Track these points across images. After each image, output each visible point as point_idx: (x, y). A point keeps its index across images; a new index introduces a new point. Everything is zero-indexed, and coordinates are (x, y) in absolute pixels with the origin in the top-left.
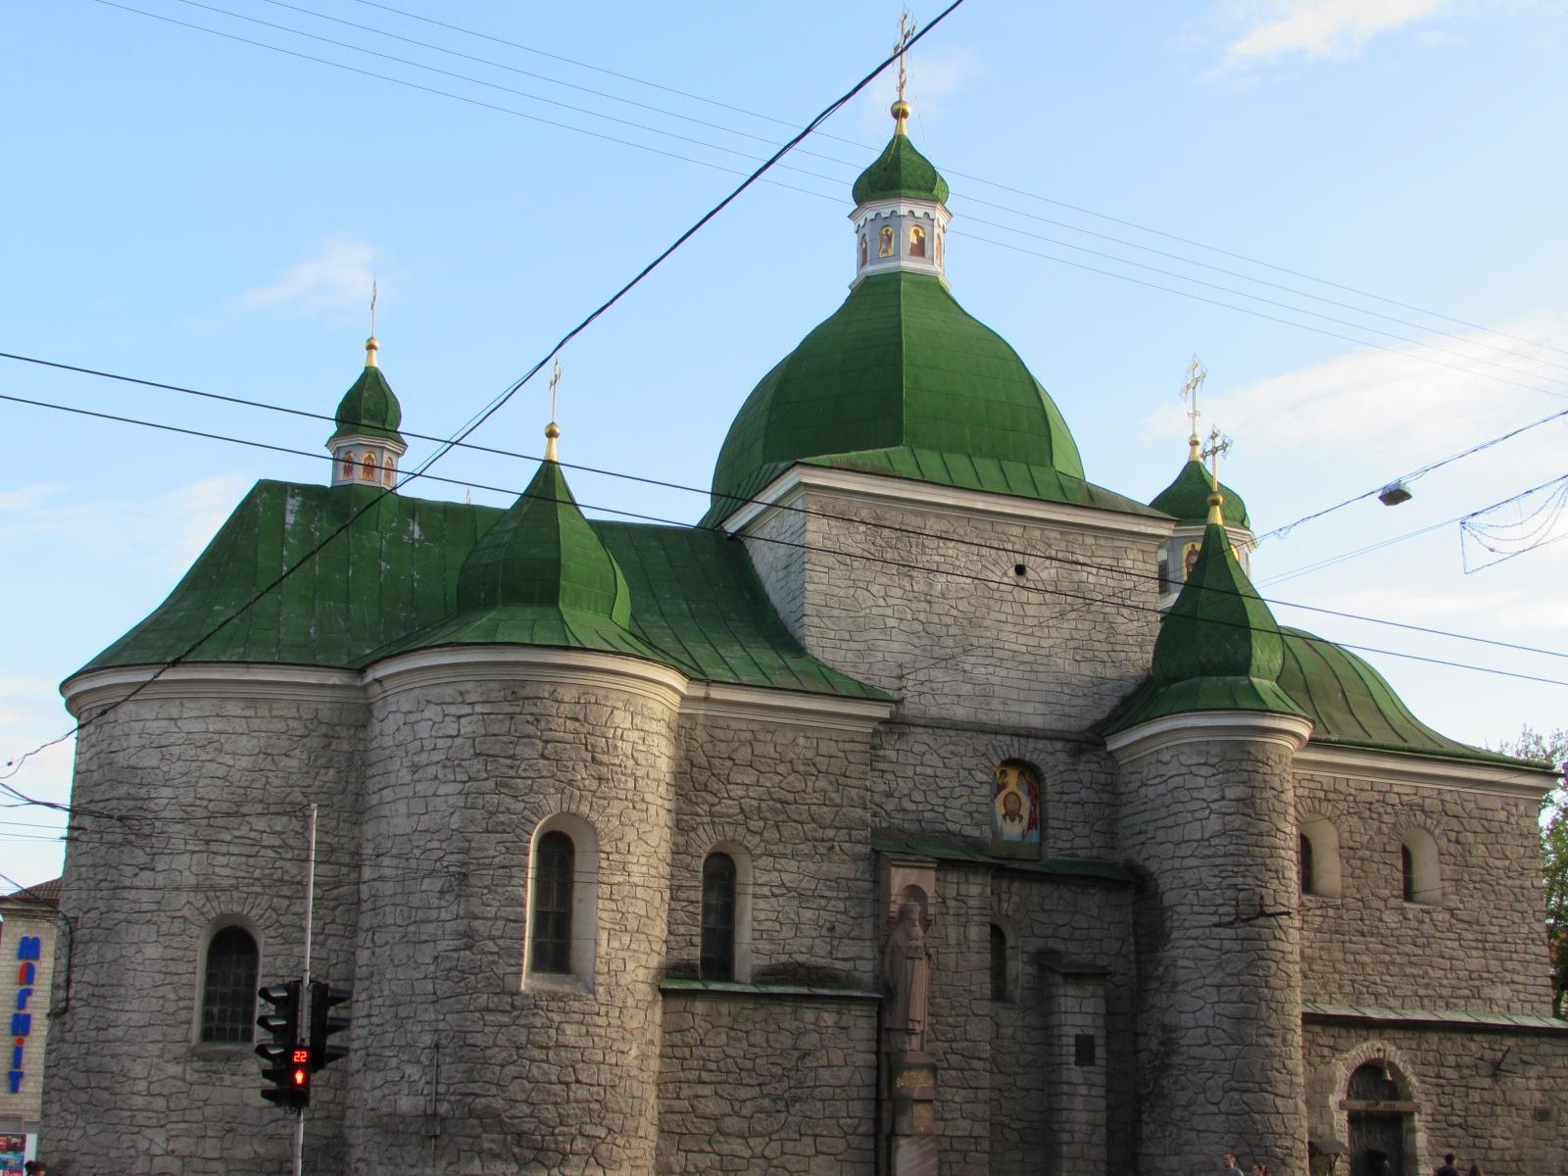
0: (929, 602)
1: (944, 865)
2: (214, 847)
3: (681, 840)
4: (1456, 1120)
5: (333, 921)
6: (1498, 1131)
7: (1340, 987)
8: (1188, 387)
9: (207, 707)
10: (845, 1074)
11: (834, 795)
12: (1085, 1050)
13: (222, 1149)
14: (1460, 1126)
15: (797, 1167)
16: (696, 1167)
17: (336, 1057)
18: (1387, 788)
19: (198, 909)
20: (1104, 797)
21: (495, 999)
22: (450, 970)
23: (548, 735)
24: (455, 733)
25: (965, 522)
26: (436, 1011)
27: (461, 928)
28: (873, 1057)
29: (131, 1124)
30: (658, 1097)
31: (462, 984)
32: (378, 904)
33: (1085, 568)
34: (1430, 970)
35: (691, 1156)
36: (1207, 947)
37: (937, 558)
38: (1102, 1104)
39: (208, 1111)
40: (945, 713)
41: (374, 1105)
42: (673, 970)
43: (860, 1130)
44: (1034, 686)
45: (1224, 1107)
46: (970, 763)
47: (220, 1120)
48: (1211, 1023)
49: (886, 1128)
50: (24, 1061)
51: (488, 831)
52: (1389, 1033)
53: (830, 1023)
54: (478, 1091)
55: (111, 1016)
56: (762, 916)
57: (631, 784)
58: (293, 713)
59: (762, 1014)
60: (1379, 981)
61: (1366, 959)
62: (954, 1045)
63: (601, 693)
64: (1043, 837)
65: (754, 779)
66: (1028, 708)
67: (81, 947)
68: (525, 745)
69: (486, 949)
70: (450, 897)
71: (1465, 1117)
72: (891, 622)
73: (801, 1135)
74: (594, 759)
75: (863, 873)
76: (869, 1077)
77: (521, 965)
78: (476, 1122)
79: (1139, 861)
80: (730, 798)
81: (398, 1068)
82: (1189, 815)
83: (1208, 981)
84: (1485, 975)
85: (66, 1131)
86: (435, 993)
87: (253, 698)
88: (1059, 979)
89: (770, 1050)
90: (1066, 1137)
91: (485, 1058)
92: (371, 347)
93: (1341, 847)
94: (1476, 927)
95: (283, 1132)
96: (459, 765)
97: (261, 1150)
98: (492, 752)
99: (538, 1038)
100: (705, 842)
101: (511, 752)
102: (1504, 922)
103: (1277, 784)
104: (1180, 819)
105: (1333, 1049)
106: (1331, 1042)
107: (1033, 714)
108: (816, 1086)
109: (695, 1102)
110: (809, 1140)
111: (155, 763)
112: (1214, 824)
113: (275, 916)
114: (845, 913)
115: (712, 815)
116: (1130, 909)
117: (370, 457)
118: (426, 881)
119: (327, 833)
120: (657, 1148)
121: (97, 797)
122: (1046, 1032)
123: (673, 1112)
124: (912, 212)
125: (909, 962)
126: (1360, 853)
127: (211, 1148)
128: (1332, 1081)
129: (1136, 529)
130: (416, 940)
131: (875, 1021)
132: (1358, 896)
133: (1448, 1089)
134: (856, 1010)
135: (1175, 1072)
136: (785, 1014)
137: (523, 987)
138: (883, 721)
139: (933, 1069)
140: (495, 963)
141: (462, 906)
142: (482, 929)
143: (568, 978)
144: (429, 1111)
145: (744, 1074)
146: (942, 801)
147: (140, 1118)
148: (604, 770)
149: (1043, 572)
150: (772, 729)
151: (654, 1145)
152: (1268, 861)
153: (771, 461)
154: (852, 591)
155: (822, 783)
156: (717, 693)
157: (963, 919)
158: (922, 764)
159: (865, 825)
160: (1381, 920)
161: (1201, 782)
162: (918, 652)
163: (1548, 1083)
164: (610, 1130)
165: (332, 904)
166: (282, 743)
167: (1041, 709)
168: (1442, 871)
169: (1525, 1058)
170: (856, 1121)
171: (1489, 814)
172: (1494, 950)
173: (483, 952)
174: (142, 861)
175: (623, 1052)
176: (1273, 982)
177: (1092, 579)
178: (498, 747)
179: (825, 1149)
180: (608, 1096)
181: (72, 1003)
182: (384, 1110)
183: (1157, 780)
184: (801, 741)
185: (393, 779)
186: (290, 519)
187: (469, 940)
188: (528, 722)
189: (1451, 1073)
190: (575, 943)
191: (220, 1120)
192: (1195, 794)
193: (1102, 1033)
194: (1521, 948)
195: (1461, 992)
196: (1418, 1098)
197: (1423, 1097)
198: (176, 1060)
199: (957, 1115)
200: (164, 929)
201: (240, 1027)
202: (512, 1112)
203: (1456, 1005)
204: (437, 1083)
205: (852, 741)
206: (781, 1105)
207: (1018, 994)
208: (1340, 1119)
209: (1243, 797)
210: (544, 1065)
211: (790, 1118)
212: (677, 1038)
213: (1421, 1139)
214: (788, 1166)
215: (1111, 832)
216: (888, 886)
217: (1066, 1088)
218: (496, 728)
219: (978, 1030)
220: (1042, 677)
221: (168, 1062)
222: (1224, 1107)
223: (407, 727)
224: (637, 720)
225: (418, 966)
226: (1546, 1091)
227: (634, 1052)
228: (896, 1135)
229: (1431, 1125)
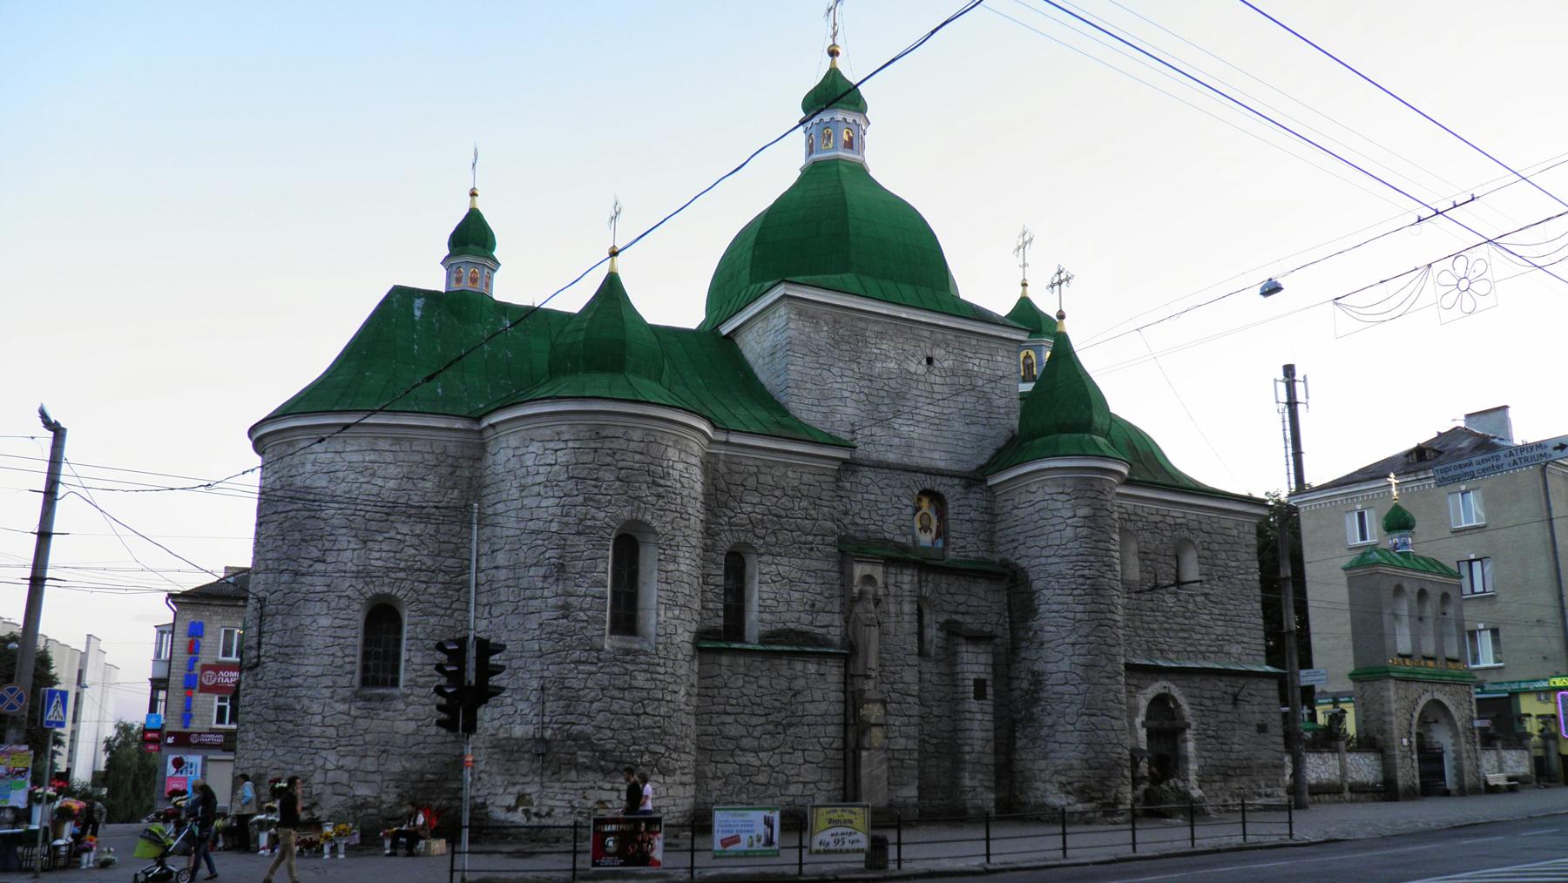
0: (870, 381)
1: (889, 562)
2: (370, 544)
3: (709, 542)
4: (1210, 732)
5: (458, 600)
6: (1236, 740)
7: (1140, 645)
8: (1019, 248)
9: (364, 443)
10: (823, 707)
11: (812, 512)
12: (980, 693)
13: (379, 765)
14: (1213, 737)
15: (792, 772)
16: (723, 773)
17: (496, 694)
18: (1166, 513)
19: (359, 591)
20: (986, 517)
21: (586, 654)
22: (551, 633)
23: (621, 464)
24: (553, 462)
25: (894, 326)
26: (542, 663)
27: (560, 603)
28: (842, 694)
29: (310, 747)
30: (696, 724)
31: (561, 643)
32: (494, 587)
33: (971, 360)
34: (1193, 634)
35: (719, 765)
36: (1065, 617)
37: (875, 351)
38: (990, 725)
39: (368, 738)
40: (882, 458)
41: (493, 732)
42: (701, 636)
43: (834, 746)
44: (940, 440)
45: (1078, 726)
46: (900, 492)
47: (377, 744)
48: (1068, 669)
49: (852, 743)
50: (193, 706)
51: (578, 533)
53: (813, 671)
54: (572, 721)
55: (294, 668)
56: (765, 596)
57: (679, 501)
58: (428, 448)
59: (767, 665)
60: (1162, 640)
61: (1155, 626)
62: (895, 686)
63: (660, 434)
64: (946, 543)
65: (759, 500)
66: (936, 455)
67: (269, 619)
68: (606, 471)
69: (579, 618)
70: (550, 580)
72: (846, 394)
73: (794, 750)
74: (654, 482)
75: (833, 566)
76: (839, 708)
77: (604, 629)
78: (572, 743)
79: (1013, 560)
80: (742, 513)
81: (512, 705)
82: (1052, 529)
83: (1066, 641)
84: (1226, 637)
85: (260, 752)
86: (540, 650)
87: (399, 436)
88: (964, 641)
89: (772, 691)
90: (967, 749)
91: (578, 697)
92: (473, 194)
93: (1139, 552)
94: (1220, 606)
95: (423, 752)
96: (556, 485)
97: (408, 765)
98: (581, 476)
99: (616, 682)
100: (726, 541)
101: (595, 476)
102: (1237, 603)
103: (1109, 508)
104: (1045, 530)
105: (1138, 687)
106: (1135, 682)
107: (939, 460)
108: (803, 716)
109: (721, 727)
110: (799, 754)
111: (324, 484)
112: (1069, 532)
113: (415, 595)
114: (821, 594)
115: (730, 524)
116: (1005, 592)
117: (474, 272)
118: (533, 569)
119: (453, 536)
120: (696, 761)
121: (280, 509)
122: (953, 678)
123: (707, 735)
124: (845, 119)
125: (867, 629)
126: (1151, 556)
127: (370, 764)
129: (1004, 335)
130: (525, 611)
131: (843, 670)
133: (1206, 713)
134: (831, 662)
135: (1043, 703)
136: (782, 665)
137: (606, 646)
138: (845, 462)
139: (884, 703)
140: (586, 628)
141: (560, 587)
142: (575, 603)
143: (637, 639)
144: (537, 736)
145: (755, 707)
146: (880, 518)
147: (316, 741)
148: (661, 490)
149: (945, 361)
150: (771, 465)
151: (694, 758)
152: (1105, 559)
153: (756, 282)
154: (819, 371)
155: (804, 504)
156: (734, 439)
157: (900, 599)
158: (867, 493)
159: (835, 533)
160: (1164, 601)
161: (1059, 505)
162: (863, 415)
163: (1264, 708)
164: (667, 748)
165: (457, 587)
166: (420, 470)
167: (943, 455)
168: (1200, 569)
170: (831, 740)
171: (1227, 532)
172: (1231, 620)
173: (576, 620)
174: (315, 555)
175: (675, 692)
176: (1110, 641)
177: (976, 368)
178: (586, 472)
179: (810, 759)
180: (666, 724)
181: (263, 659)
182: (502, 734)
183: (1028, 504)
184: (790, 474)
185: (504, 497)
186: (417, 313)
187: (565, 610)
188: (608, 454)
189: (1208, 703)
190: (640, 613)
191: (377, 744)
192: (1055, 513)
193: (989, 678)
194: (1246, 620)
195: (1211, 649)
197: (1191, 718)
198: (344, 700)
199: (897, 734)
200: (333, 605)
201: (390, 677)
202: (601, 736)
204: (543, 715)
205: (824, 475)
206: (780, 729)
207: (933, 651)
208: (1142, 734)
209: (1090, 514)
210: (621, 702)
211: (787, 738)
212: (708, 682)
213: (1191, 746)
214: (786, 771)
215: (991, 542)
216: (851, 576)
217: (968, 715)
218: (585, 458)
219: (910, 676)
220: (944, 434)
221: (337, 701)
222: (1078, 726)
223: (515, 459)
224: (683, 456)
225: (526, 631)
227: (682, 692)
228: (860, 749)
229: (1198, 737)
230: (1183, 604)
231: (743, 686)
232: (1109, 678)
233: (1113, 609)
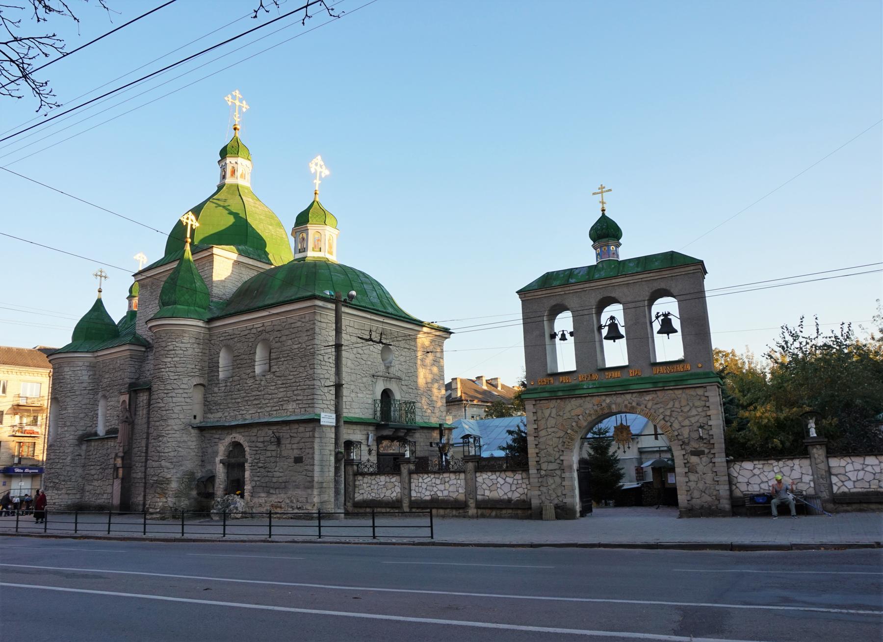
4: (260, 465)
6: (277, 469)
14: (262, 467)
18: (252, 327)
52: (238, 430)
60: (243, 408)
61: (239, 400)
62: (140, 448)
84: (285, 399)
94: (283, 378)
126: (241, 357)
128: (216, 453)
133: (259, 452)
139: (123, 458)
150: (113, 360)
160: (246, 383)
163: (301, 445)
164: (59, 479)
169: (291, 434)
171: (293, 326)
184: (118, 362)
189: (261, 445)
194: (302, 384)
195: (275, 408)
196: (248, 456)
203: (272, 414)
213: (247, 474)
226: (301, 449)
227: (69, 458)
230: (257, 382)
231: (96, 454)
232: (154, 439)
233: (160, 401)
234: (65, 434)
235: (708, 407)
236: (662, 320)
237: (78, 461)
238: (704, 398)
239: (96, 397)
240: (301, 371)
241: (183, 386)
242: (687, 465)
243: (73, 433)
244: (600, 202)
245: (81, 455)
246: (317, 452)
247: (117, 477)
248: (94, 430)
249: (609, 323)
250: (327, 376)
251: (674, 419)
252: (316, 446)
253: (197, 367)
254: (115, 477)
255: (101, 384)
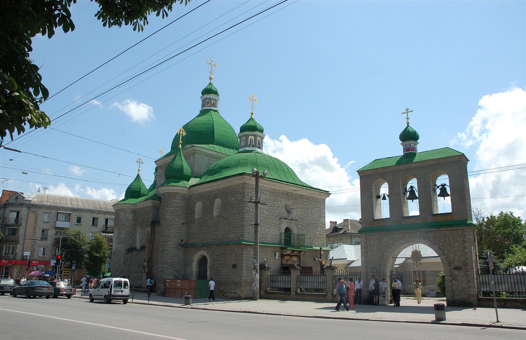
4: (215, 268)
14: (216, 270)
63: (119, 210)
71: (217, 267)
84: (228, 232)
128: (192, 261)
132: (205, 218)
139: (148, 261)
172: (231, 225)
189: (215, 257)
194: (237, 223)
195: (223, 237)
227: (122, 261)
230: (215, 222)
234: (120, 248)
235: (465, 241)
236: (441, 188)
237: (127, 263)
238: (463, 236)
239: (136, 228)
240: (237, 216)
241: (176, 224)
242: (452, 276)
243: (124, 247)
244: (406, 118)
245: (128, 260)
246: (244, 262)
247: (145, 272)
248: (135, 246)
249: (410, 190)
250: (252, 219)
251: (444, 248)
252: (244, 259)
253: (183, 213)
254: (144, 272)
255: (138, 221)
